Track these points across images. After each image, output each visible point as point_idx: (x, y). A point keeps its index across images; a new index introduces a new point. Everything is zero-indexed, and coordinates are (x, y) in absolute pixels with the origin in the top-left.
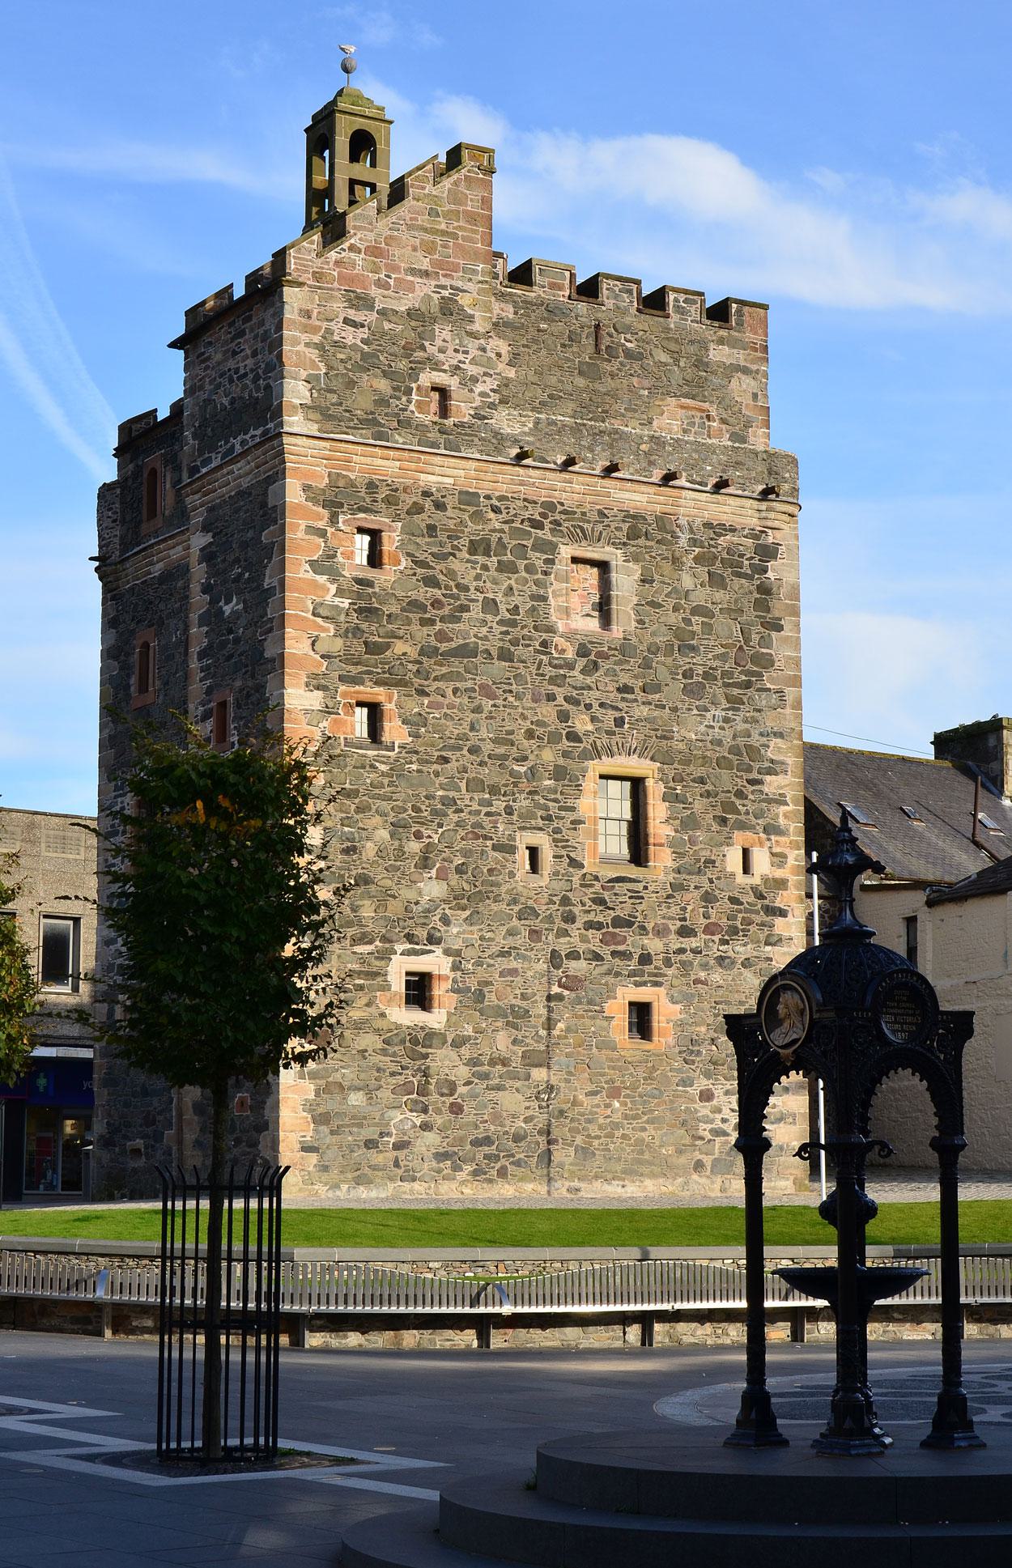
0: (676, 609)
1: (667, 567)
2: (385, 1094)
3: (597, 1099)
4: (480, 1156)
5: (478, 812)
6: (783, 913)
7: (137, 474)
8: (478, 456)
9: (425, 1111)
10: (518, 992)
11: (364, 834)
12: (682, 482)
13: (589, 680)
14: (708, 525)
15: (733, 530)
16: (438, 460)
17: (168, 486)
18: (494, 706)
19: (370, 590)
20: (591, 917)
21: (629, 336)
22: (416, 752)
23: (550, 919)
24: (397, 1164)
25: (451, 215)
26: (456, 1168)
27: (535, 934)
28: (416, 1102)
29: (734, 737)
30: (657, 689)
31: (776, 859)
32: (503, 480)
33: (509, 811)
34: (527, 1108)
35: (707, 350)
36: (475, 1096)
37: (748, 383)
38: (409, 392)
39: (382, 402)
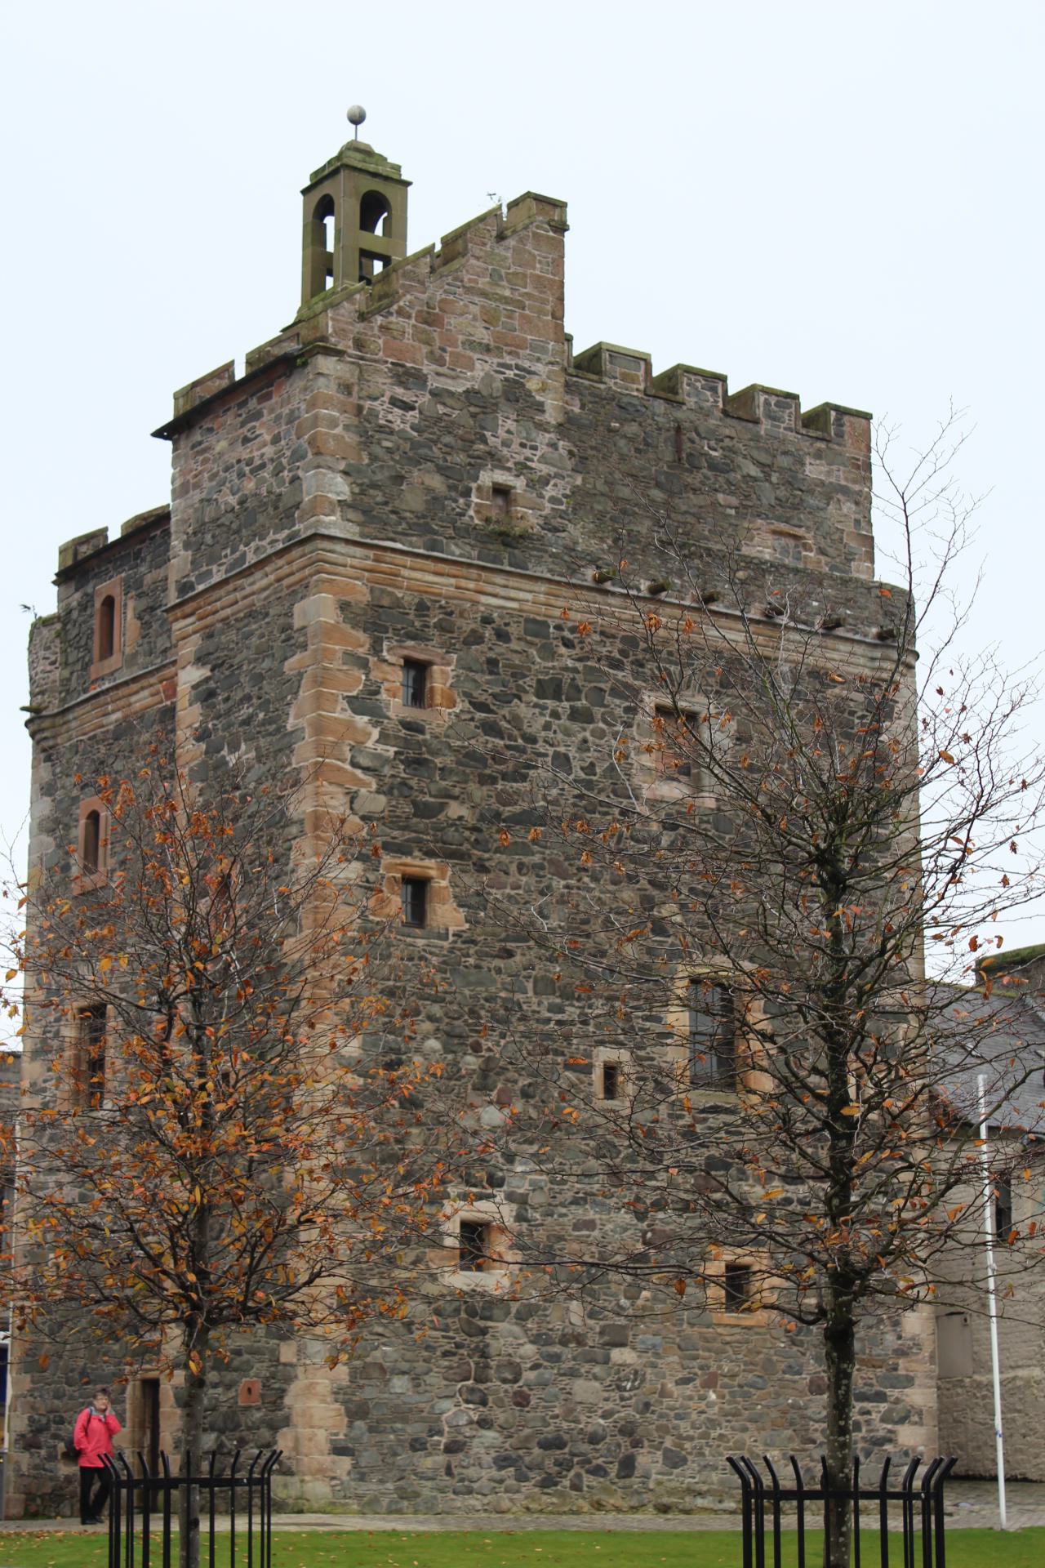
2: (434, 1379)
3: (688, 1390)
4: (549, 1463)
5: (549, 1020)
7: (84, 606)
8: (548, 576)
9: (484, 1403)
10: (594, 1249)
11: (413, 1044)
12: (784, 620)
16: (499, 579)
17: (130, 614)
18: (567, 887)
19: (421, 737)
21: (713, 443)
22: (474, 942)
24: (449, 1471)
25: (514, 279)
26: (521, 1478)
28: (472, 1390)
32: (578, 609)
34: (607, 1399)
35: (803, 464)
36: (544, 1384)
37: (848, 507)
38: (467, 493)
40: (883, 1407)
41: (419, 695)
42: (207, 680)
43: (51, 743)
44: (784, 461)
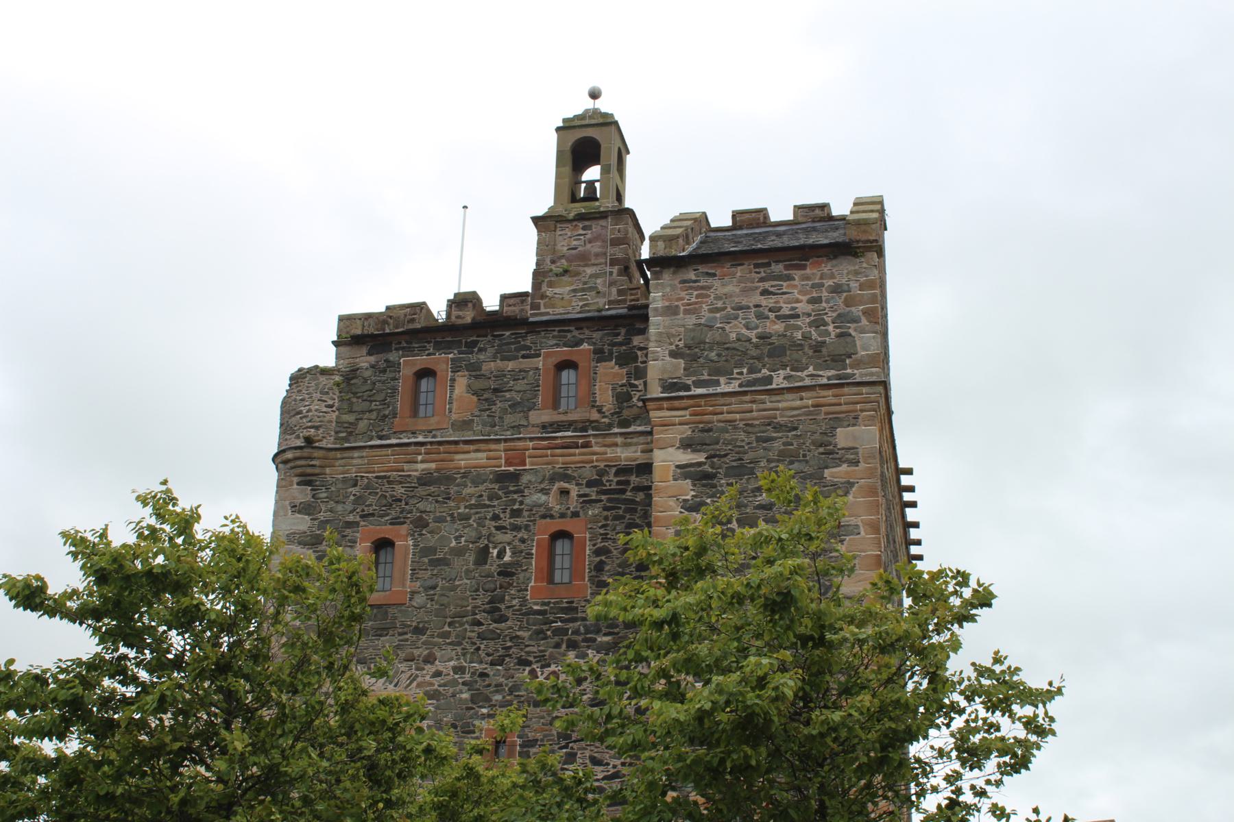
42: (700, 464)
43: (317, 471)
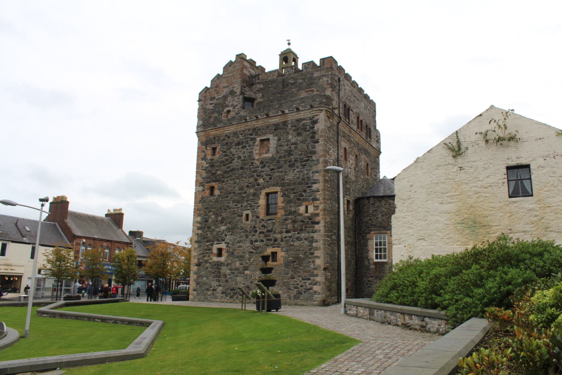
0: (287, 145)
1: (285, 135)
6: (318, 223)
13: (263, 169)
14: (297, 120)
15: (304, 119)
20: (261, 231)
23: (250, 232)
27: (247, 236)
29: (303, 176)
30: (281, 167)
31: (316, 208)
32: (242, 127)
33: (242, 207)
39: (216, 118)
40: (310, 281)
41: (214, 154)
44: (309, 76)
